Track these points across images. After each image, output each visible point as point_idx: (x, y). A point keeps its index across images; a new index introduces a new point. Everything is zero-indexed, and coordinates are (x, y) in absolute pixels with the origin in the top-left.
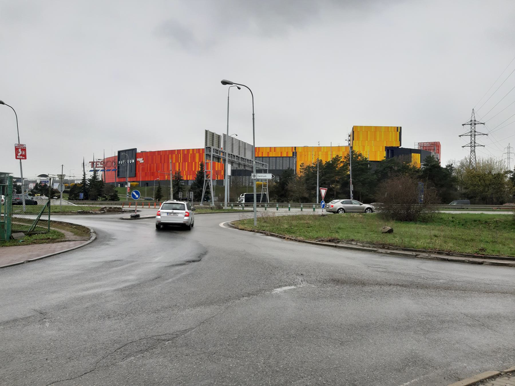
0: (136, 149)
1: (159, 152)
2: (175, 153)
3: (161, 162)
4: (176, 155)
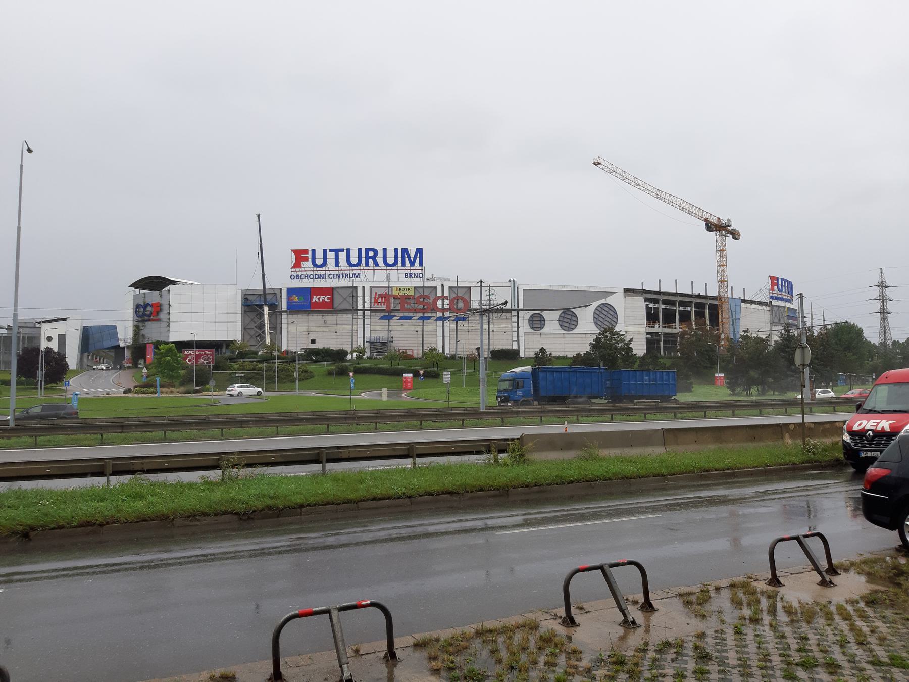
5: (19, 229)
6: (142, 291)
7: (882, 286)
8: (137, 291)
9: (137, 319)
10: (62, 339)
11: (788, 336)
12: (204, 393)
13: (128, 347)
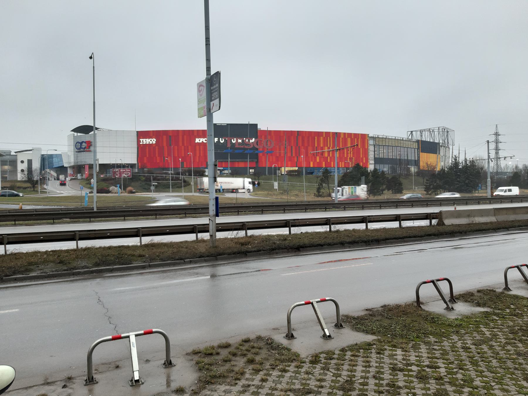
0: (256, 125)
1: (299, 132)
2: (322, 135)
3: (303, 145)
4: (324, 139)
5: (94, 102)
6: (79, 134)
7: (497, 134)
8: (76, 134)
9: (77, 150)
10: (30, 162)
11: (456, 162)
12: (137, 194)
13: (70, 167)
